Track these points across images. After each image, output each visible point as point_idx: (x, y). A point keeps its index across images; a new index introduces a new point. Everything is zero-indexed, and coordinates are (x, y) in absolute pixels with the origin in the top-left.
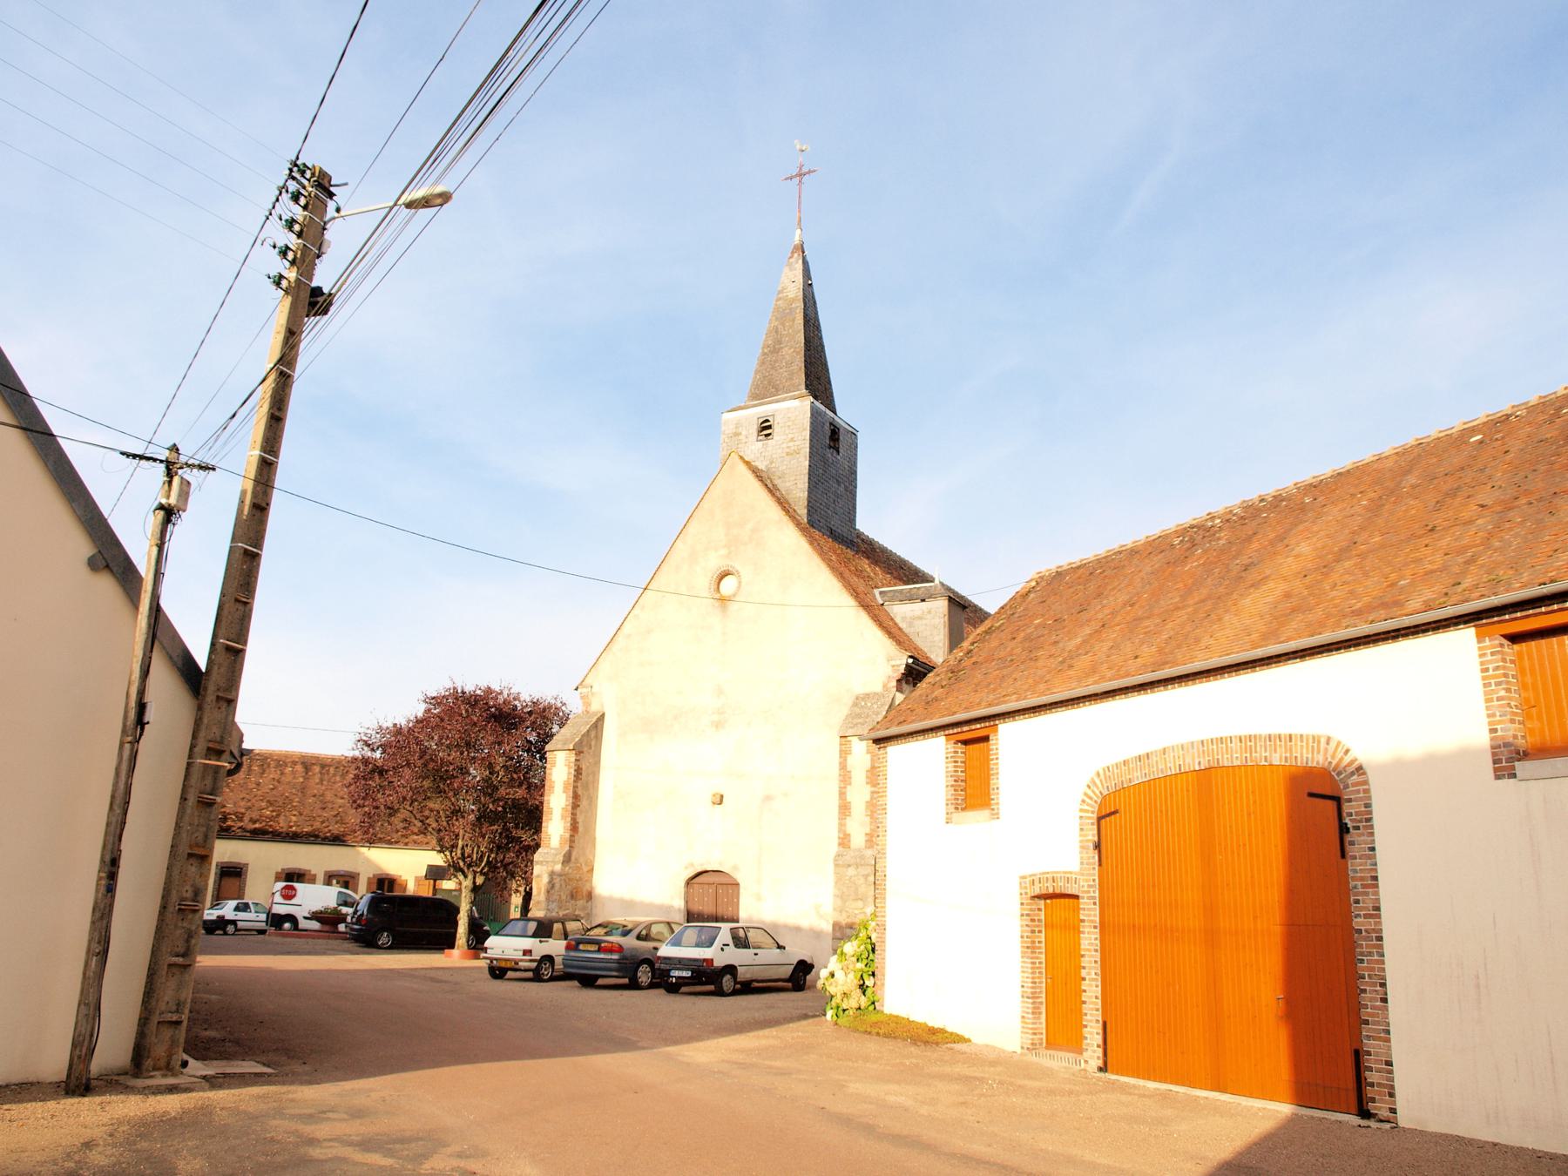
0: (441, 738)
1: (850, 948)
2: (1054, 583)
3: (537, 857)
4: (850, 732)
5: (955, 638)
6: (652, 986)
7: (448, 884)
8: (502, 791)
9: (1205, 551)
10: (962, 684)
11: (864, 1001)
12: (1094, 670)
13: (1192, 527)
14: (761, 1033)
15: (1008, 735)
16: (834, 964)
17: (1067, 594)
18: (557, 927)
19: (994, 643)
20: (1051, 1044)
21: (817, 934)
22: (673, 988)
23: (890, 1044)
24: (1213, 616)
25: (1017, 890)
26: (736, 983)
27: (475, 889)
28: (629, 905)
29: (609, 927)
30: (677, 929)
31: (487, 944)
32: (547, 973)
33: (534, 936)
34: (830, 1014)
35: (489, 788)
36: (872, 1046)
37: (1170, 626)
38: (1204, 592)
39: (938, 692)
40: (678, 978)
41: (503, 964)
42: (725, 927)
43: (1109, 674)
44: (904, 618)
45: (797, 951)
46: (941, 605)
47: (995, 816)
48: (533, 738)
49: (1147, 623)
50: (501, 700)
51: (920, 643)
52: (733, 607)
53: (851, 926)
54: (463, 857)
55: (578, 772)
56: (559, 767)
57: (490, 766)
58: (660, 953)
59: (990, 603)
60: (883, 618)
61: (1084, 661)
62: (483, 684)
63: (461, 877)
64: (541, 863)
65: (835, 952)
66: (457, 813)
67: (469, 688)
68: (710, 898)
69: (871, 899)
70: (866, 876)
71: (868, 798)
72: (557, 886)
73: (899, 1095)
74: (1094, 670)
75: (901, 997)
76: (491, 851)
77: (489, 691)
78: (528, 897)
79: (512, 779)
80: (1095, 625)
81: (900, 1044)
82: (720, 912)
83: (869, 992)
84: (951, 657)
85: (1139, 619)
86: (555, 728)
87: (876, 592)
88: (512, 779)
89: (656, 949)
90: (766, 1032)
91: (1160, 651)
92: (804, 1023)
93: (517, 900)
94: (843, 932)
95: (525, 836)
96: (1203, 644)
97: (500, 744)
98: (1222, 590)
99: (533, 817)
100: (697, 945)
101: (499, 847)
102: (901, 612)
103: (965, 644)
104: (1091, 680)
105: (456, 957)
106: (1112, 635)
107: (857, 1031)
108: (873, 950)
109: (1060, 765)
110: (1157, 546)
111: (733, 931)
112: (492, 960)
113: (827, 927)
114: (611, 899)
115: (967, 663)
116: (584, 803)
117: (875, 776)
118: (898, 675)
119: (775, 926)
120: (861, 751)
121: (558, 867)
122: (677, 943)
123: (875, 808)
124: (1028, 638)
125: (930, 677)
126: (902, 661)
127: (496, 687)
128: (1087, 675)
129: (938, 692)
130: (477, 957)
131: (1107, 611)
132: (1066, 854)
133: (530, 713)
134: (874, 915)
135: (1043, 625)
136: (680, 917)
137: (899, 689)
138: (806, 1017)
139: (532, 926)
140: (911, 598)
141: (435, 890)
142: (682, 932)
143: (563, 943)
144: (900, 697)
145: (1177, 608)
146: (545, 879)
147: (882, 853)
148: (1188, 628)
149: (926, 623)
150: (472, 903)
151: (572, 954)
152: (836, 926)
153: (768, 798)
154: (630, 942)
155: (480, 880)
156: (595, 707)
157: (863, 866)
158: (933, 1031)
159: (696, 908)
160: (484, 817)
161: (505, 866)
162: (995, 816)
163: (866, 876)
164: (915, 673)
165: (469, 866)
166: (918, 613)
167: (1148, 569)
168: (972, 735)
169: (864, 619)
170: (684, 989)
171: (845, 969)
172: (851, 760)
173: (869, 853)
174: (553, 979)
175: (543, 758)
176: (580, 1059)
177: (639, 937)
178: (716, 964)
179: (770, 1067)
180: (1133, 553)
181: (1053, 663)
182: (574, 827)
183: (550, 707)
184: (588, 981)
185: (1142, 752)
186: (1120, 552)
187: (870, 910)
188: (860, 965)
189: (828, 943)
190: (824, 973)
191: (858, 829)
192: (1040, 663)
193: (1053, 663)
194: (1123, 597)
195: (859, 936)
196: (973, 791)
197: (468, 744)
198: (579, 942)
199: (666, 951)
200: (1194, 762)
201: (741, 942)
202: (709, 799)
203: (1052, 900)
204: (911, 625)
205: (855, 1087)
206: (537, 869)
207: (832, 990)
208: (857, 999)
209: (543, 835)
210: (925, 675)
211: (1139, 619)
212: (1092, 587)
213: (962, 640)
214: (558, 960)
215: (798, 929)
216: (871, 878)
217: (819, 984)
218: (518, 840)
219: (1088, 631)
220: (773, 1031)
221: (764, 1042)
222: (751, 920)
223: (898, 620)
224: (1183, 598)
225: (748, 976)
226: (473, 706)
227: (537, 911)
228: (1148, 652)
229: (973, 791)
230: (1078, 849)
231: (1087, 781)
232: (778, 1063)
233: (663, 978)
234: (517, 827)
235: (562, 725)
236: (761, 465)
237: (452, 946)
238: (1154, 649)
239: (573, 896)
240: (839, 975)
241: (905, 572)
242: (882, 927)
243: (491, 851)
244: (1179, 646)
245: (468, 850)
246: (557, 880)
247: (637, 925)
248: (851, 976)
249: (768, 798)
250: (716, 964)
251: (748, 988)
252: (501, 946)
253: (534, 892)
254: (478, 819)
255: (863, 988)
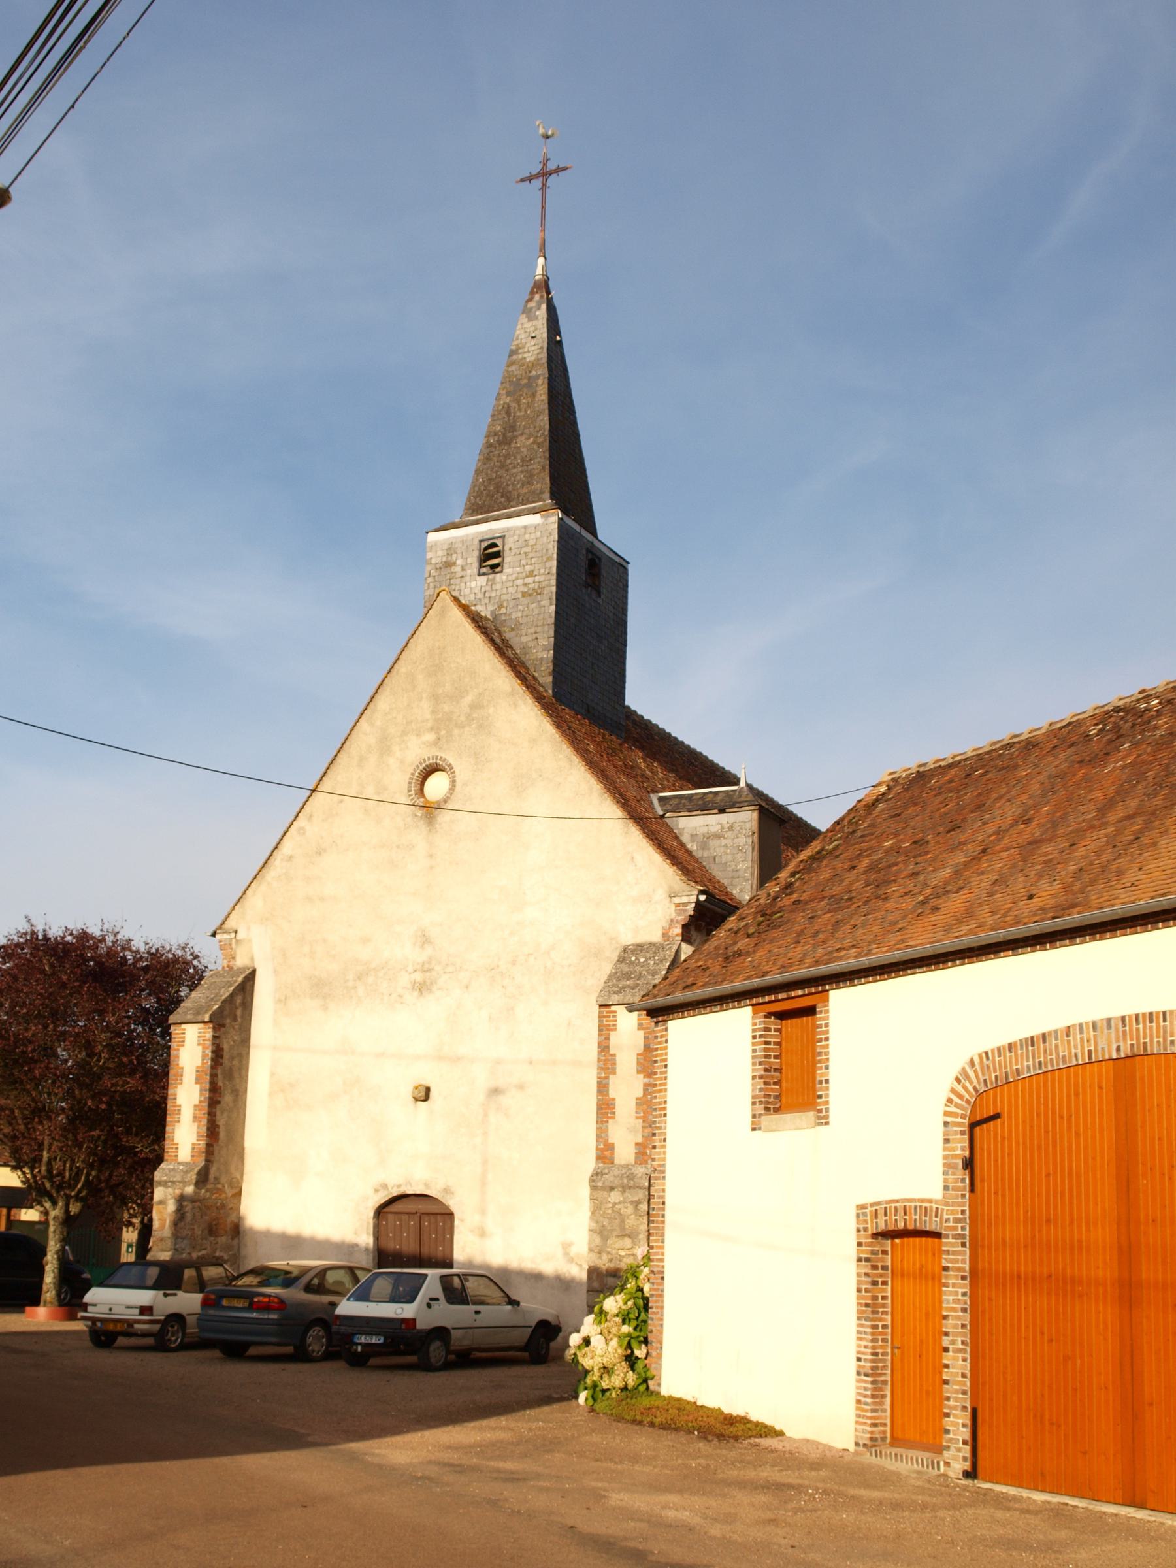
0: (13, 1007)
1: (612, 1304)
2: (914, 789)
3: (158, 1175)
4: (615, 999)
5: (768, 867)
6: (328, 1356)
7: (29, 1215)
8: (107, 1082)
9: (1135, 745)
10: (776, 933)
11: (632, 1379)
12: (969, 914)
13: (1117, 710)
14: (485, 1423)
15: (844, 1005)
16: (589, 1326)
17: (931, 805)
18: (189, 1273)
19: (825, 874)
20: (896, 1441)
21: (563, 1284)
22: (360, 1361)
23: (668, 1439)
24: (1145, 840)
25: (852, 1224)
26: (448, 1352)
27: (68, 1221)
28: (293, 1243)
29: (267, 1275)
30: (363, 1277)
31: (89, 1297)
32: (176, 1340)
33: (154, 1287)
34: (583, 1396)
35: (86, 1076)
36: (642, 1441)
37: (1080, 852)
38: (1133, 804)
39: (743, 943)
40: (364, 1345)
41: (111, 1327)
42: (433, 1274)
43: (990, 921)
44: (693, 837)
45: (537, 1307)
46: (748, 819)
47: (823, 1119)
48: (150, 1003)
49: (1047, 848)
50: (103, 948)
51: (717, 872)
52: (443, 818)
53: (615, 1273)
54: (50, 1176)
55: (217, 1055)
56: (190, 1048)
57: (89, 1046)
58: (339, 1311)
59: (821, 817)
60: (664, 835)
61: (955, 903)
62: (76, 925)
63: (48, 1205)
64: (164, 1184)
65: (590, 1311)
66: (40, 1112)
67: (55, 932)
68: (412, 1229)
69: (643, 1236)
70: (636, 1204)
71: (640, 1094)
72: (189, 1216)
73: (680, 1509)
74: (969, 913)
75: (682, 1375)
76: (91, 1166)
77: (84, 936)
78: (146, 1231)
79: (121, 1064)
80: (973, 849)
81: (683, 1437)
82: (426, 1251)
83: (639, 1365)
84: (762, 894)
85: (1036, 843)
86: (184, 991)
87: (654, 798)
88: (121, 1064)
89: (334, 1305)
90: (492, 1422)
91: (1066, 888)
92: (546, 1409)
93: (130, 1236)
94: (603, 1281)
95: (141, 1147)
96: (1127, 880)
97: (102, 1013)
98: (1158, 802)
99: (153, 1118)
100: (394, 1299)
101: (103, 1161)
102: (691, 827)
103: (783, 875)
104: (965, 929)
105: (40, 1317)
106: (997, 864)
107: (620, 1419)
108: (646, 1307)
109: (913, 1047)
110: (1068, 737)
111: (445, 1281)
112: (94, 1320)
113: (579, 1273)
114: (267, 1234)
115: (786, 901)
116: (227, 1098)
117: (651, 1062)
118: (683, 918)
119: (505, 1272)
120: (628, 1024)
121: (190, 1189)
122: (363, 1296)
123: (651, 1108)
124: (872, 868)
125: (732, 922)
126: (690, 897)
127: (95, 931)
128: (960, 922)
129: (743, 943)
130: (72, 1317)
131: (990, 829)
132: (918, 1170)
133: (146, 969)
134: (648, 1258)
135: (896, 849)
136: (365, 1261)
137: (686, 938)
138: (548, 1400)
139: (153, 1272)
140: (703, 807)
141: (10, 1222)
142: (370, 1282)
143: (198, 1297)
144: (687, 950)
145: (1093, 827)
146: (171, 1206)
147: (660, 1171)
148: (1107, 856)
149: (726, 840)
150: (65, 1241)
151: (212, 1312)
152: (593, 1272)
153: (495, 1092)
154: (295, 1294)
155: (74, 1209)
156: (241, 961)
157: (631, 1189)
158: (731, 1420)
159: (392, 1245)
160: (80, 1118)
161: (113, 1190)
162: (823, 1119)
163: (636, 1204)
164: (708, 917)
165: (59, 1188)
166: (715, 829)
167: (1052, 770)
168: (791, 1006)
169: (635, 835)
170: (373, 1361)
171: (606, 1336)
172: (614, 1038)
173: (640, 1170)
174: (184, 1347)
175: (166, 1033)
176: (225, 1460)
177: (309, 1288)
178: (420, 1325)
179: (498, 1471)
180: (1029, 746)
181: (909, 903)
182: (212, 1132)
183: (176, 960)
184: (235, 1351)
185: (1036, 1031)
186: (1011, 745)
187: (641, 1251)
188: (626, 1329)
189: (582, 1298)
190: (575, 1339)
191: (625, 1139)
192: (889, 905)
193: (909, 903)
194: (1011, 811)
195: (624, 1287)
196: (789, 1084)
197: (54, 1014)
198: (221, 1295)
199: (348, 1307)
200: (1109, 1047)
201: (455, 1293)
202: (407, 1092)
203: (895, 1237)
204: (704, 846)
205: (618, 1498)
206: (159, 1193)
207: (586, 1362)
208: (623, 1377)
209: (167, 1144)
210: (723, 919)
211: (1036, 843)
212: (969, 796)
213: (779, 868)
214: (191, 1320)
215: (537, 1277)
216: (644, 1207)
217: (569, 1354)
218: (131, 1151)
219: (960, 858)
220: (503, 1421)
221: (489, 1436)
222: (470, 1264)
223: (685, 839)
224: (1102, 811)
225: (466, 1343)
226: (59, 959)
227: (161, 1252)
228: (1048, 892)
229: (789, 1084)
230: (940, 1169)
231: (955, 1071)
232: (509, 1465)
233: (342, 1344)
234: (128, 1132)
235: (193, 987)
236: (485, 611)
237: (36, 1303)
238: (1057, 886)
239: (212, 1230)
240: (597, 1341)
241: (695, 769)
242: (659, 1276)
243: (91, 1166)
244: (1093, 882)
245: (57, 1165)
246: (188, 1207)
247: (305, 1271)
248: (614, 1343)
249: (495, 1092)
250: (420, 1325)
251: (466, 1359)
252: (109, 1300)
253: (156, 1224)
254: (71, 1121)
255: (631, 1360)
